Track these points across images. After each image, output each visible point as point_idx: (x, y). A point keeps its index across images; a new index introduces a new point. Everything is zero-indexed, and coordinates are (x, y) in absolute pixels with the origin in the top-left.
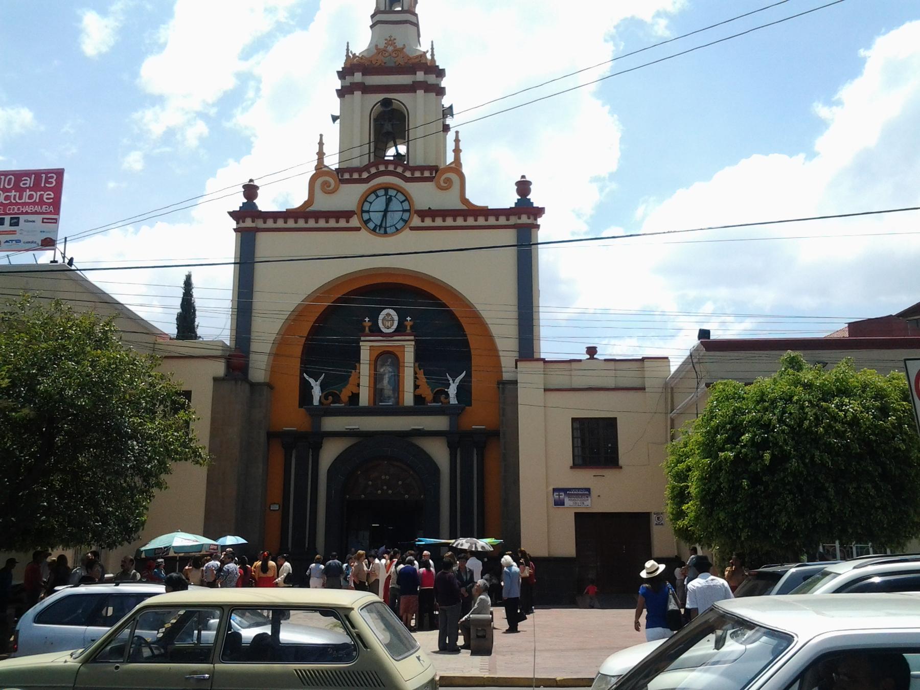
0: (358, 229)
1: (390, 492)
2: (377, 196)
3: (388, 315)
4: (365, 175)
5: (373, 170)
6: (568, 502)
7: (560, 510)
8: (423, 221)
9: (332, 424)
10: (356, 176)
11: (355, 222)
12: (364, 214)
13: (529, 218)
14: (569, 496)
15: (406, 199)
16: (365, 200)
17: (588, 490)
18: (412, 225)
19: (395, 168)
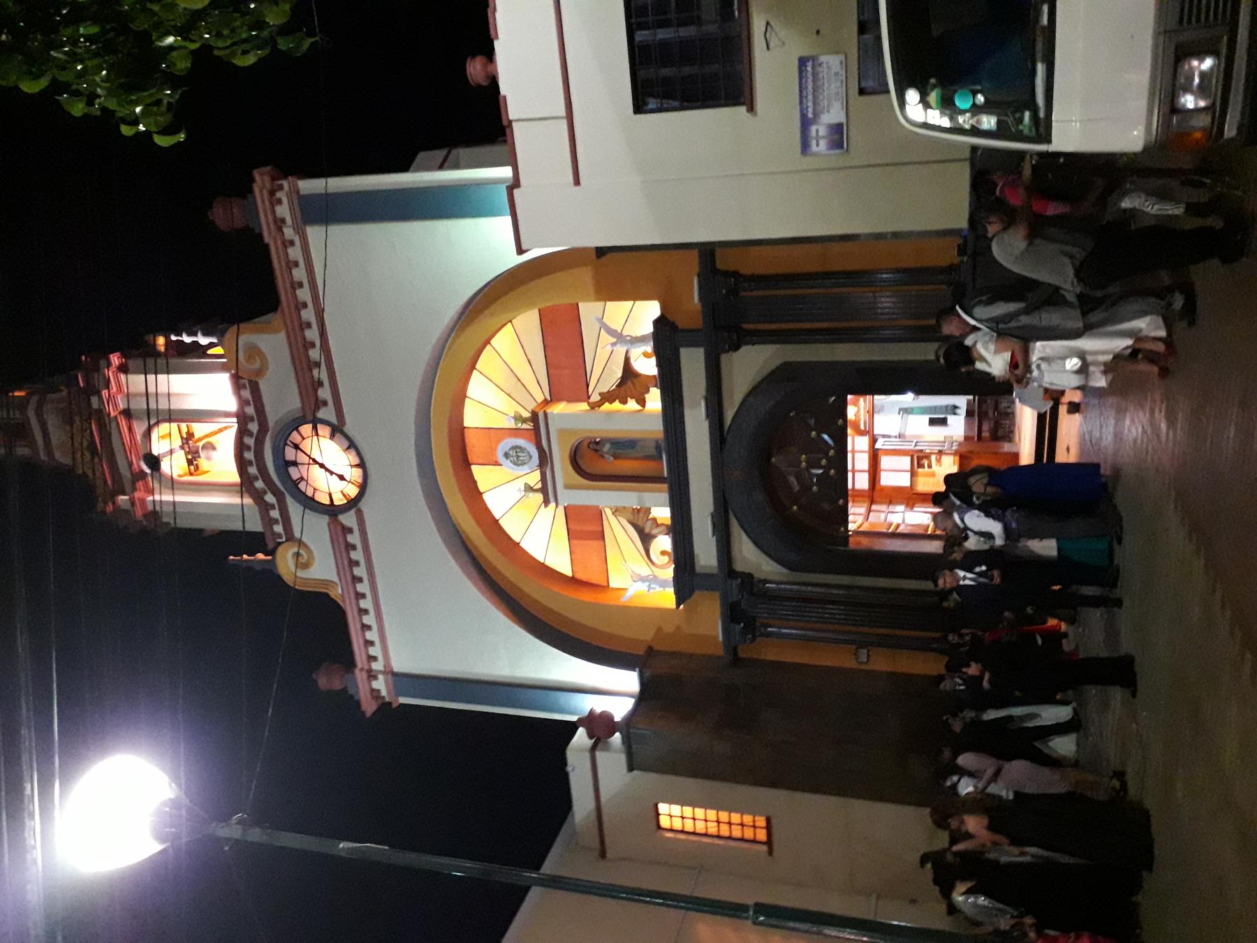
0: (360, 514)
1: (832, 452)
2: (302, 479)
3: (506, 455)
4: (270, 498)
5: (259, 484)
6: (834, 114)
7: (856, 136)
8: (325, 403)
9: (706, 554)
10: (275, 514)
11: (348, 519)
12: (337, 503)
13: (279, 202)
14: (816, 114)
15: (296, 429)
16: (312, 499)
17: (802, 62)
18: (334, 420)
19: (249, 448)
